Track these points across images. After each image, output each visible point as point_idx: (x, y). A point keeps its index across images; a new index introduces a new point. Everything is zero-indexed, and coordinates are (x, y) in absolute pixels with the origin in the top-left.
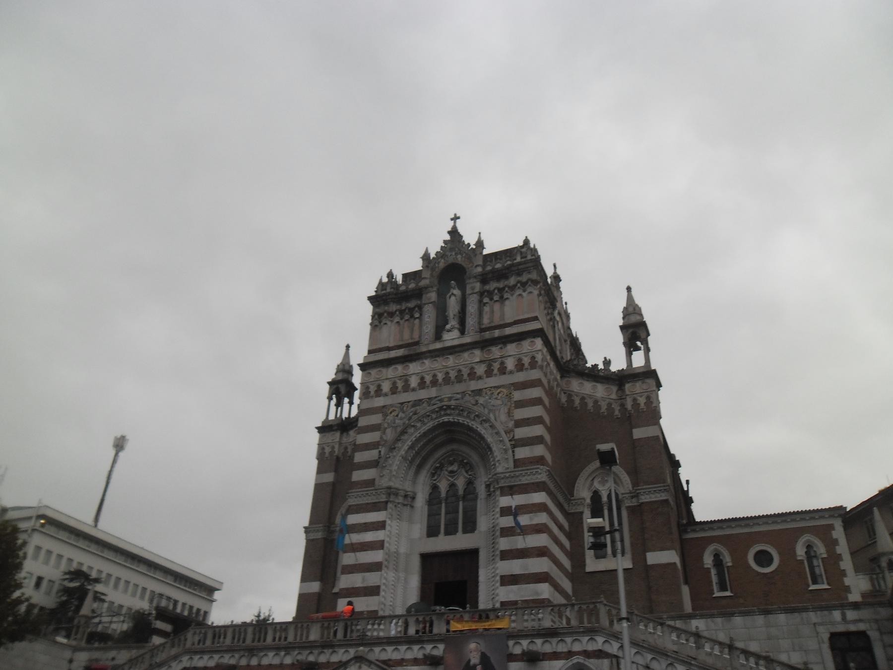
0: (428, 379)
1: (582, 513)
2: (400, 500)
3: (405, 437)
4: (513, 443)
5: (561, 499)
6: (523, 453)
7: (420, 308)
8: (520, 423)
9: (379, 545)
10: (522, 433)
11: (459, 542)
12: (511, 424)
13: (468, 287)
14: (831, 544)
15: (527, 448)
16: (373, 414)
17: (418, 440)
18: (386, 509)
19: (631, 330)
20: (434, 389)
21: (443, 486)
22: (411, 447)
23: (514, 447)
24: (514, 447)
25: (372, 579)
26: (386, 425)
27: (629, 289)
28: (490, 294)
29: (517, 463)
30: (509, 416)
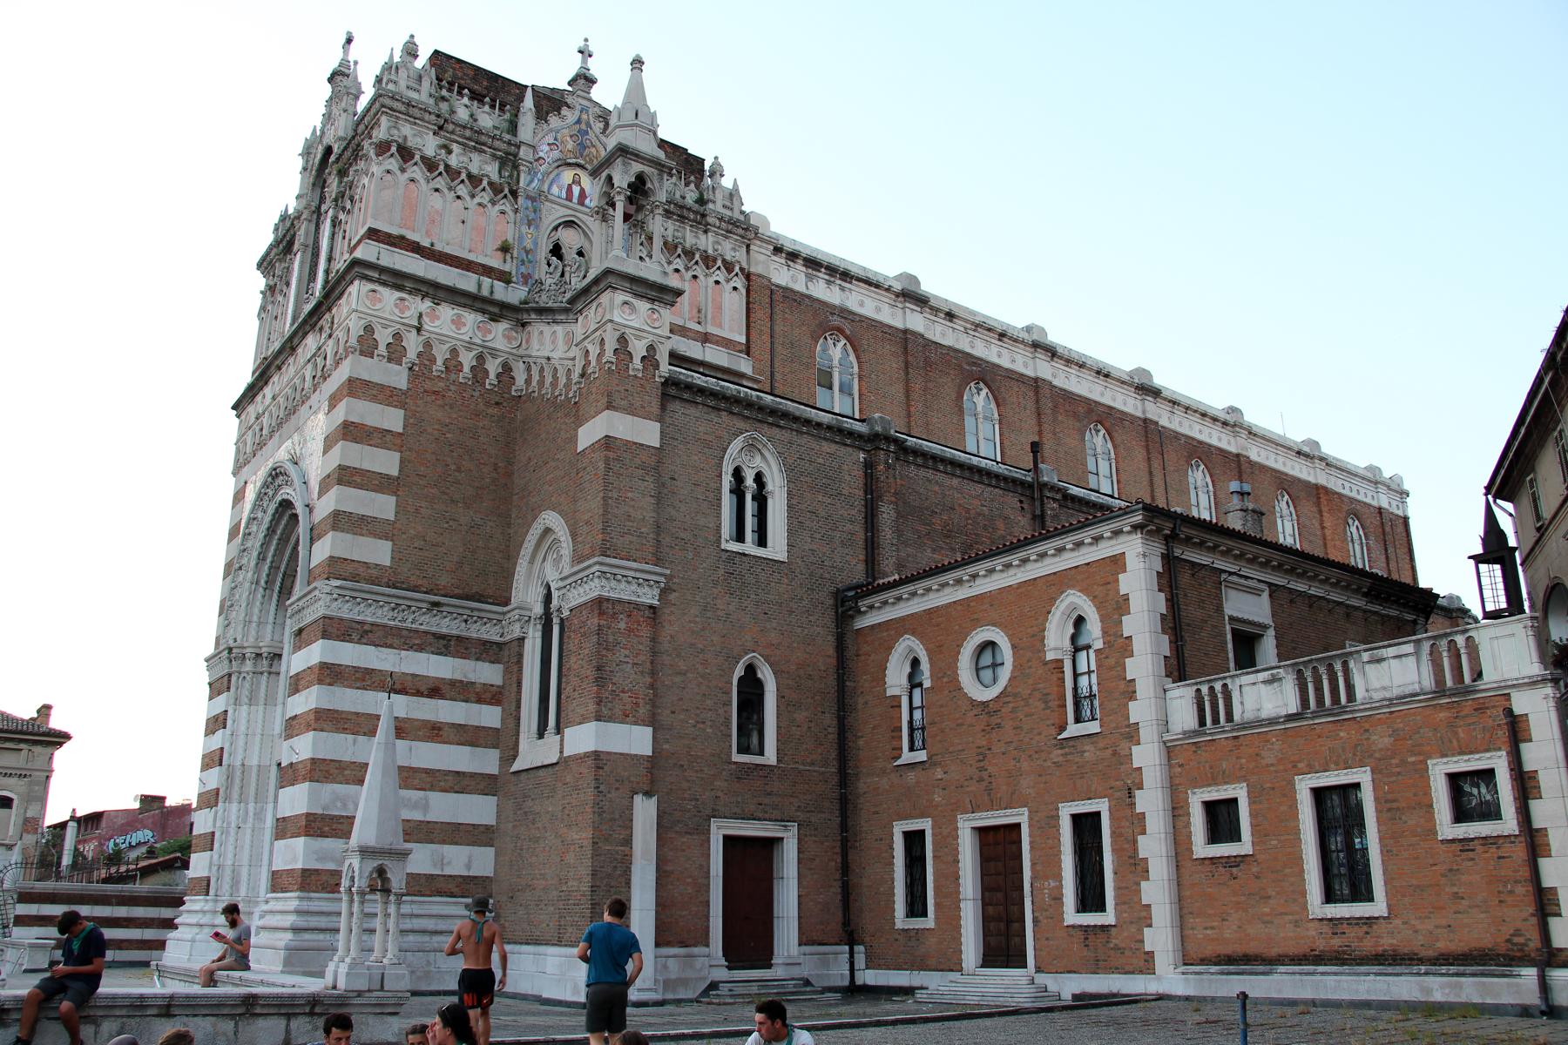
1: (522, 640)
2: (248, 666)
3: (249, 544)
5: (446, 625)
14: (1114, 608)
17: (265, 545)
19: (604, 175)
22: (261, 558)
27: (637, 63)
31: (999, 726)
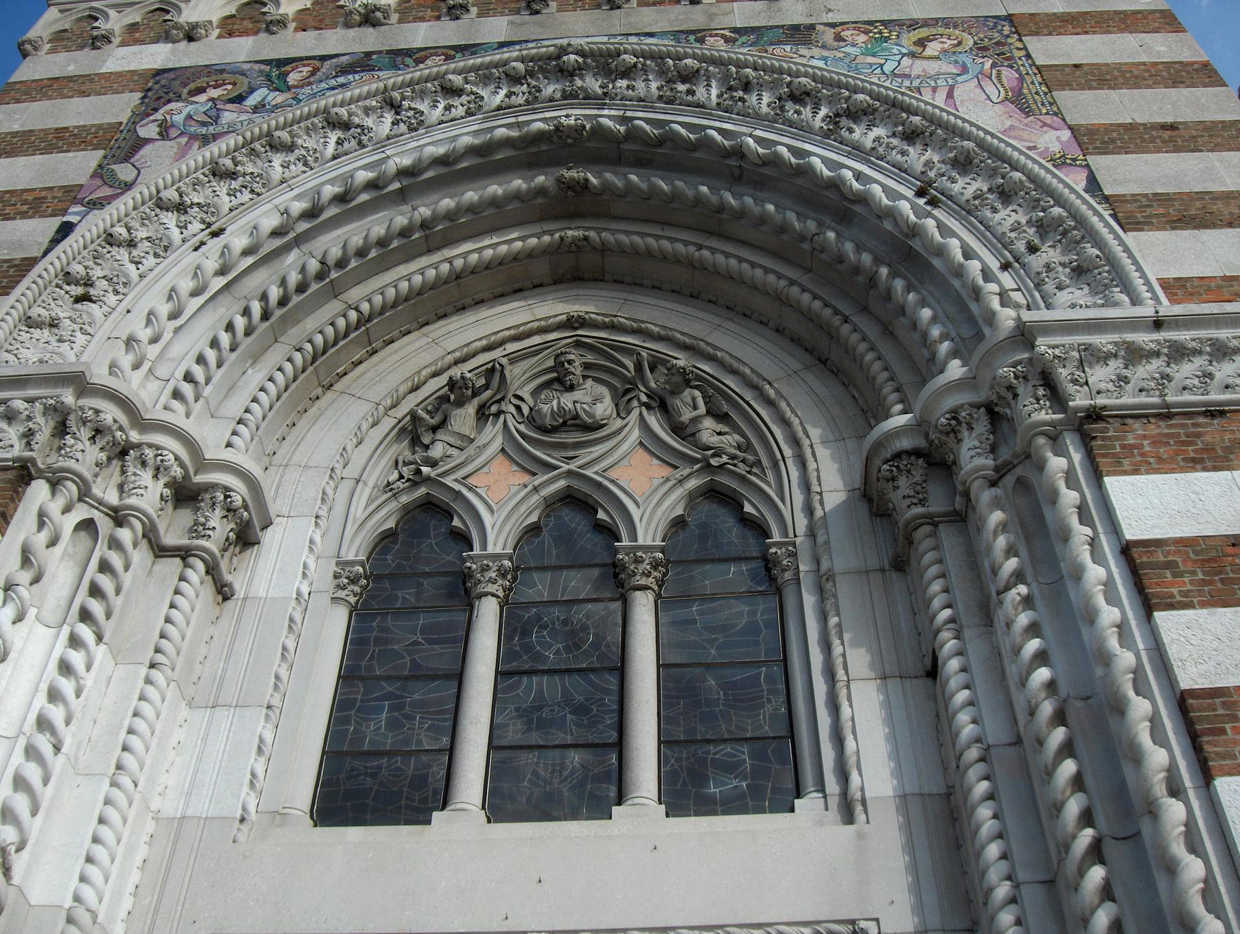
16: (84, 94)
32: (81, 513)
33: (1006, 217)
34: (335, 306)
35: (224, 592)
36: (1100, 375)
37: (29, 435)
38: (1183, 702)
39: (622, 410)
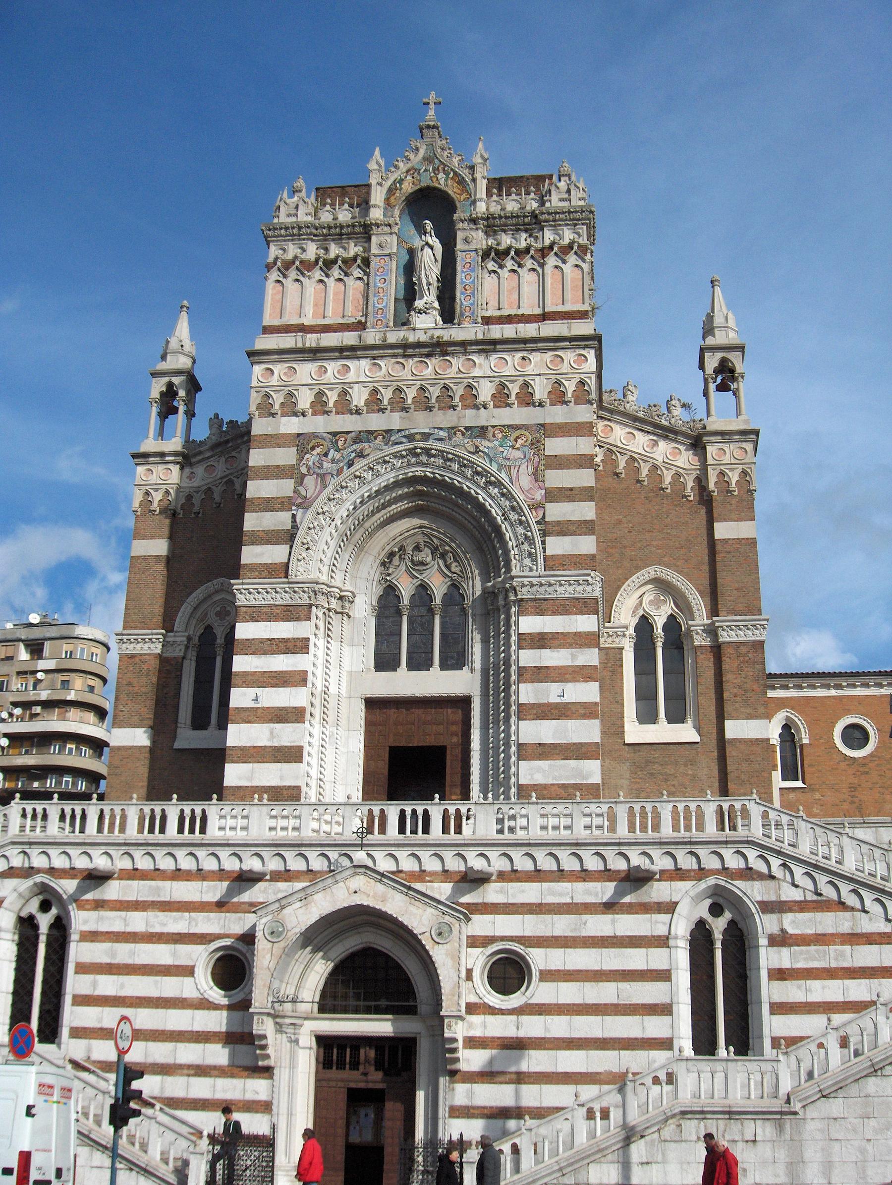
0: (387, 395)
1: (622, 648)
4: (542, 527)
6: (557, 546)
7: (367, 262)
8: (553, 495)
9: (299, 679)
10: (556, 511)
11: (437, 682)
12: (539, 495)
13: (460, 235)
15: (567, 539)
16: (279, 446)
18: (308, 619)
19: (719, 355)
20: (397, 415)
21: (406, 588)
23: (544, 534)
24: (544, 534)
25: (285, 735)
26: (304, 470)
28: (501, 255)
29: (551, 563)
30: (536, 481)
31: (867, 773)
32: (323, 611)
33: (520, 530)
34: (362, 530)
35: (349, 616)
36: (525, 590)
37: (310, 597)
38: (519, 668)
39: (434, 559)
